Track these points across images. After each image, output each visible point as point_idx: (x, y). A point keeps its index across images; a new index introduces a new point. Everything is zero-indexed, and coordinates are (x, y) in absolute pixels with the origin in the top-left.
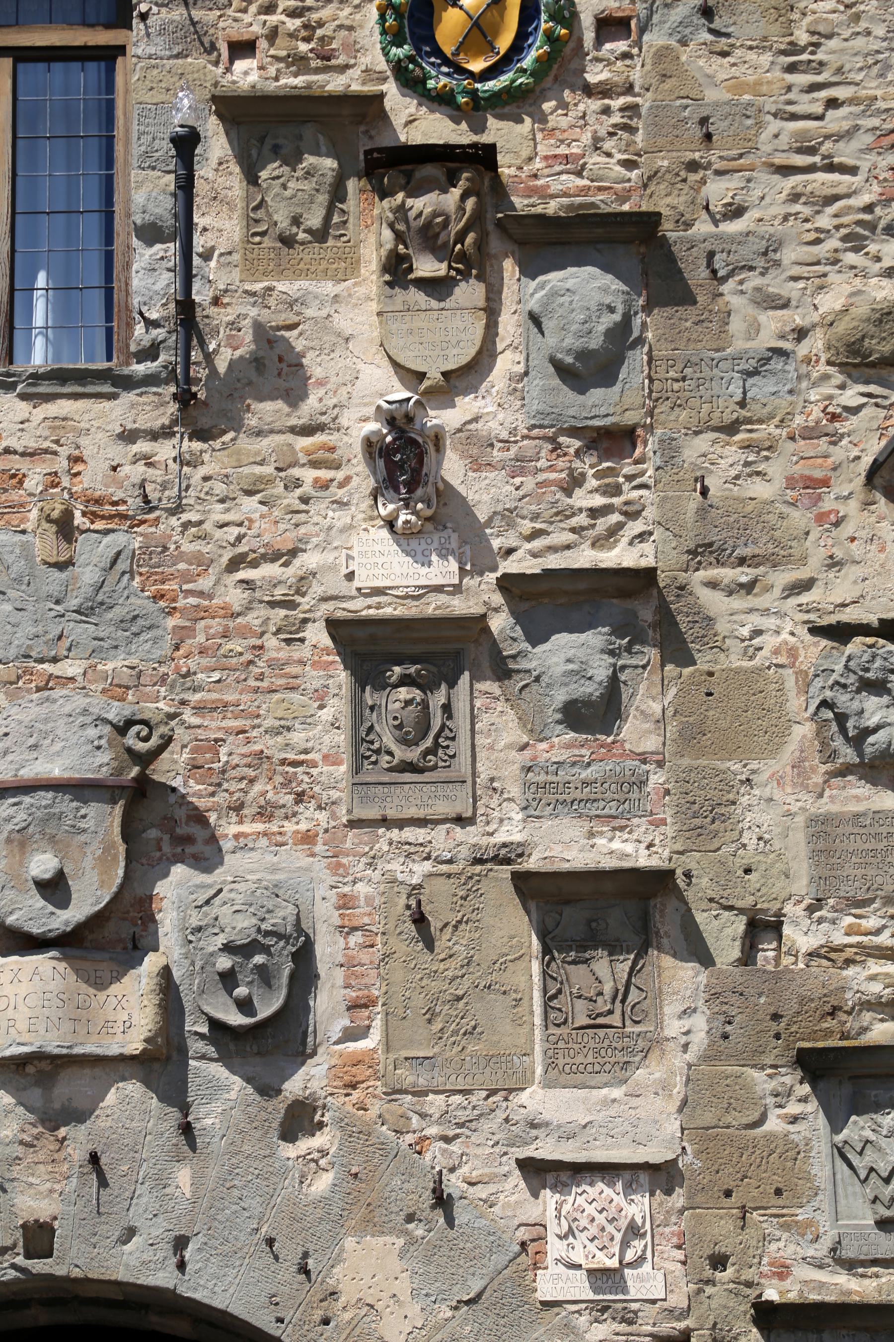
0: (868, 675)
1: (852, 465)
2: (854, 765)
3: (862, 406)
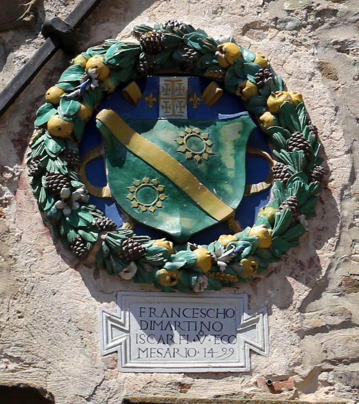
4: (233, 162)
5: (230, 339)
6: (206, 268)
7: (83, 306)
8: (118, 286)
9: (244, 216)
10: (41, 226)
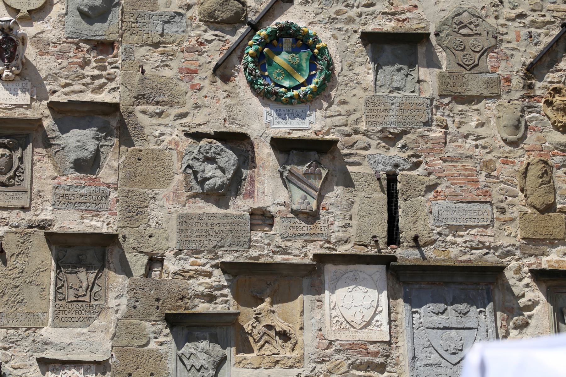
1: (207, 65)
2: (199, 193)
3: (214, 40)
4: (305, 65)
5: (304, 119)
6: (297, 97)
7: (259, 109)
8: (270, 103)
9: (309, 81)
10: (246, 84)
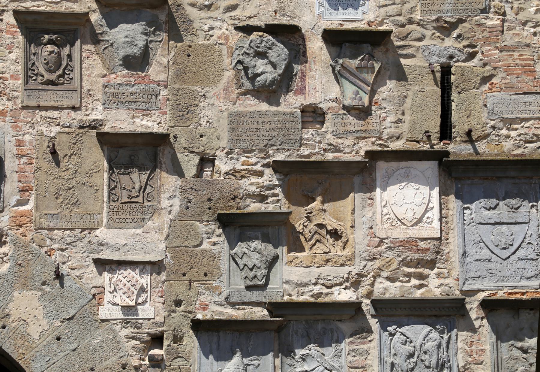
0: (259, 50)
